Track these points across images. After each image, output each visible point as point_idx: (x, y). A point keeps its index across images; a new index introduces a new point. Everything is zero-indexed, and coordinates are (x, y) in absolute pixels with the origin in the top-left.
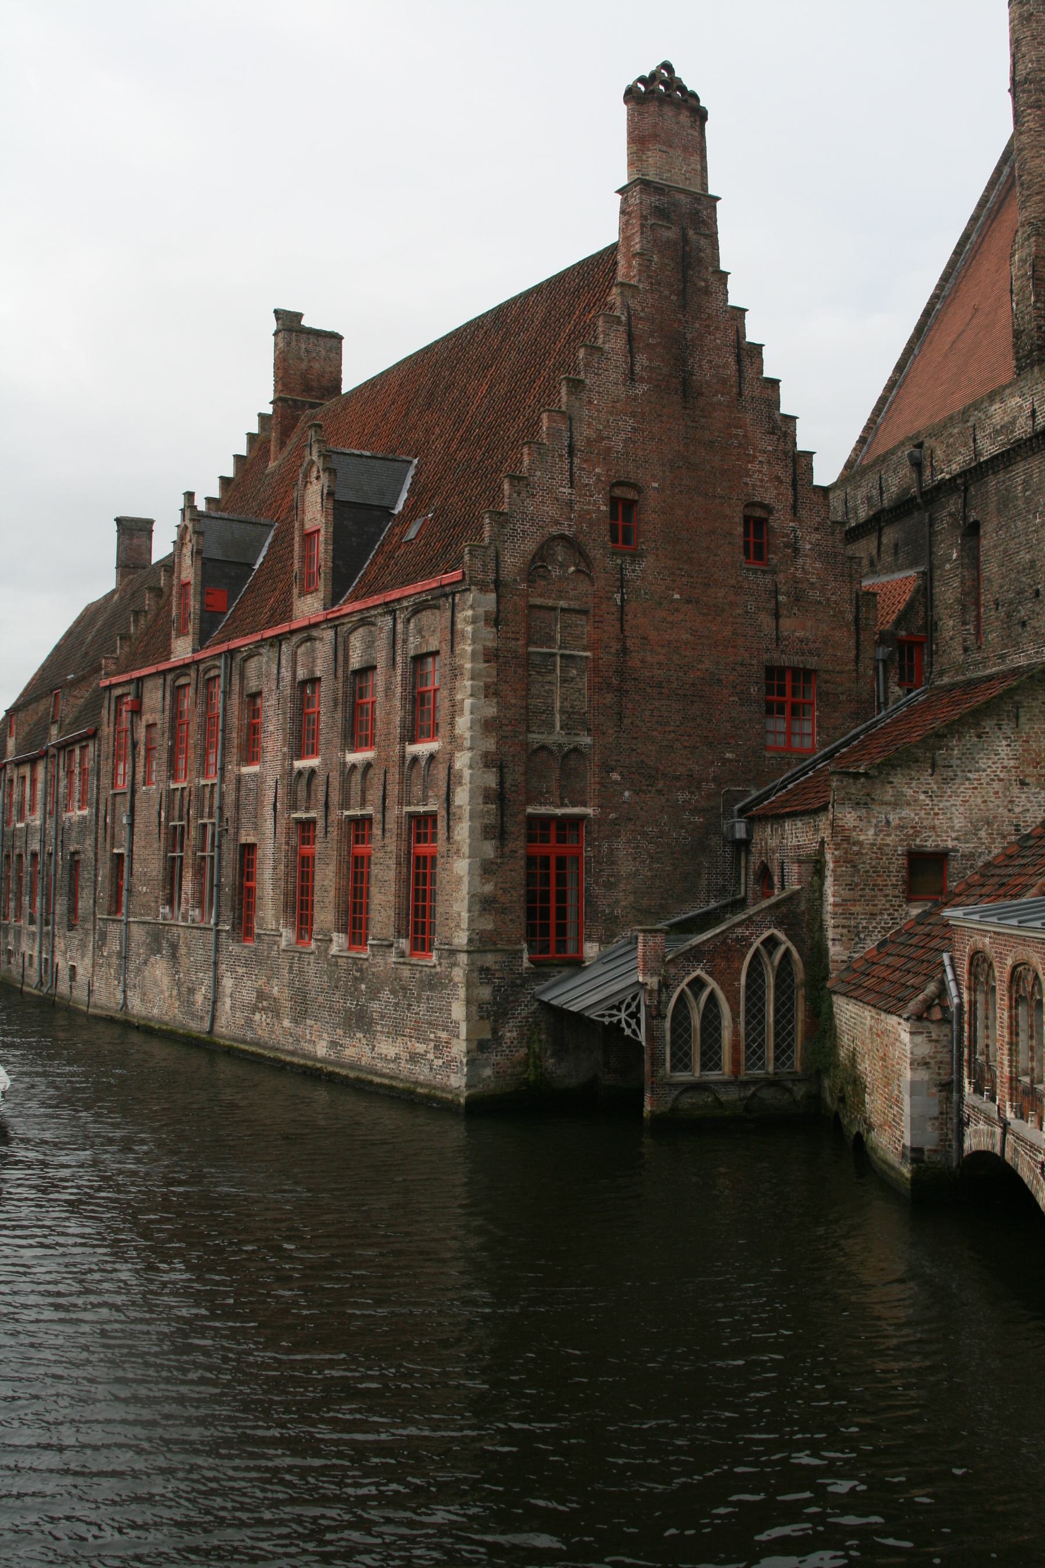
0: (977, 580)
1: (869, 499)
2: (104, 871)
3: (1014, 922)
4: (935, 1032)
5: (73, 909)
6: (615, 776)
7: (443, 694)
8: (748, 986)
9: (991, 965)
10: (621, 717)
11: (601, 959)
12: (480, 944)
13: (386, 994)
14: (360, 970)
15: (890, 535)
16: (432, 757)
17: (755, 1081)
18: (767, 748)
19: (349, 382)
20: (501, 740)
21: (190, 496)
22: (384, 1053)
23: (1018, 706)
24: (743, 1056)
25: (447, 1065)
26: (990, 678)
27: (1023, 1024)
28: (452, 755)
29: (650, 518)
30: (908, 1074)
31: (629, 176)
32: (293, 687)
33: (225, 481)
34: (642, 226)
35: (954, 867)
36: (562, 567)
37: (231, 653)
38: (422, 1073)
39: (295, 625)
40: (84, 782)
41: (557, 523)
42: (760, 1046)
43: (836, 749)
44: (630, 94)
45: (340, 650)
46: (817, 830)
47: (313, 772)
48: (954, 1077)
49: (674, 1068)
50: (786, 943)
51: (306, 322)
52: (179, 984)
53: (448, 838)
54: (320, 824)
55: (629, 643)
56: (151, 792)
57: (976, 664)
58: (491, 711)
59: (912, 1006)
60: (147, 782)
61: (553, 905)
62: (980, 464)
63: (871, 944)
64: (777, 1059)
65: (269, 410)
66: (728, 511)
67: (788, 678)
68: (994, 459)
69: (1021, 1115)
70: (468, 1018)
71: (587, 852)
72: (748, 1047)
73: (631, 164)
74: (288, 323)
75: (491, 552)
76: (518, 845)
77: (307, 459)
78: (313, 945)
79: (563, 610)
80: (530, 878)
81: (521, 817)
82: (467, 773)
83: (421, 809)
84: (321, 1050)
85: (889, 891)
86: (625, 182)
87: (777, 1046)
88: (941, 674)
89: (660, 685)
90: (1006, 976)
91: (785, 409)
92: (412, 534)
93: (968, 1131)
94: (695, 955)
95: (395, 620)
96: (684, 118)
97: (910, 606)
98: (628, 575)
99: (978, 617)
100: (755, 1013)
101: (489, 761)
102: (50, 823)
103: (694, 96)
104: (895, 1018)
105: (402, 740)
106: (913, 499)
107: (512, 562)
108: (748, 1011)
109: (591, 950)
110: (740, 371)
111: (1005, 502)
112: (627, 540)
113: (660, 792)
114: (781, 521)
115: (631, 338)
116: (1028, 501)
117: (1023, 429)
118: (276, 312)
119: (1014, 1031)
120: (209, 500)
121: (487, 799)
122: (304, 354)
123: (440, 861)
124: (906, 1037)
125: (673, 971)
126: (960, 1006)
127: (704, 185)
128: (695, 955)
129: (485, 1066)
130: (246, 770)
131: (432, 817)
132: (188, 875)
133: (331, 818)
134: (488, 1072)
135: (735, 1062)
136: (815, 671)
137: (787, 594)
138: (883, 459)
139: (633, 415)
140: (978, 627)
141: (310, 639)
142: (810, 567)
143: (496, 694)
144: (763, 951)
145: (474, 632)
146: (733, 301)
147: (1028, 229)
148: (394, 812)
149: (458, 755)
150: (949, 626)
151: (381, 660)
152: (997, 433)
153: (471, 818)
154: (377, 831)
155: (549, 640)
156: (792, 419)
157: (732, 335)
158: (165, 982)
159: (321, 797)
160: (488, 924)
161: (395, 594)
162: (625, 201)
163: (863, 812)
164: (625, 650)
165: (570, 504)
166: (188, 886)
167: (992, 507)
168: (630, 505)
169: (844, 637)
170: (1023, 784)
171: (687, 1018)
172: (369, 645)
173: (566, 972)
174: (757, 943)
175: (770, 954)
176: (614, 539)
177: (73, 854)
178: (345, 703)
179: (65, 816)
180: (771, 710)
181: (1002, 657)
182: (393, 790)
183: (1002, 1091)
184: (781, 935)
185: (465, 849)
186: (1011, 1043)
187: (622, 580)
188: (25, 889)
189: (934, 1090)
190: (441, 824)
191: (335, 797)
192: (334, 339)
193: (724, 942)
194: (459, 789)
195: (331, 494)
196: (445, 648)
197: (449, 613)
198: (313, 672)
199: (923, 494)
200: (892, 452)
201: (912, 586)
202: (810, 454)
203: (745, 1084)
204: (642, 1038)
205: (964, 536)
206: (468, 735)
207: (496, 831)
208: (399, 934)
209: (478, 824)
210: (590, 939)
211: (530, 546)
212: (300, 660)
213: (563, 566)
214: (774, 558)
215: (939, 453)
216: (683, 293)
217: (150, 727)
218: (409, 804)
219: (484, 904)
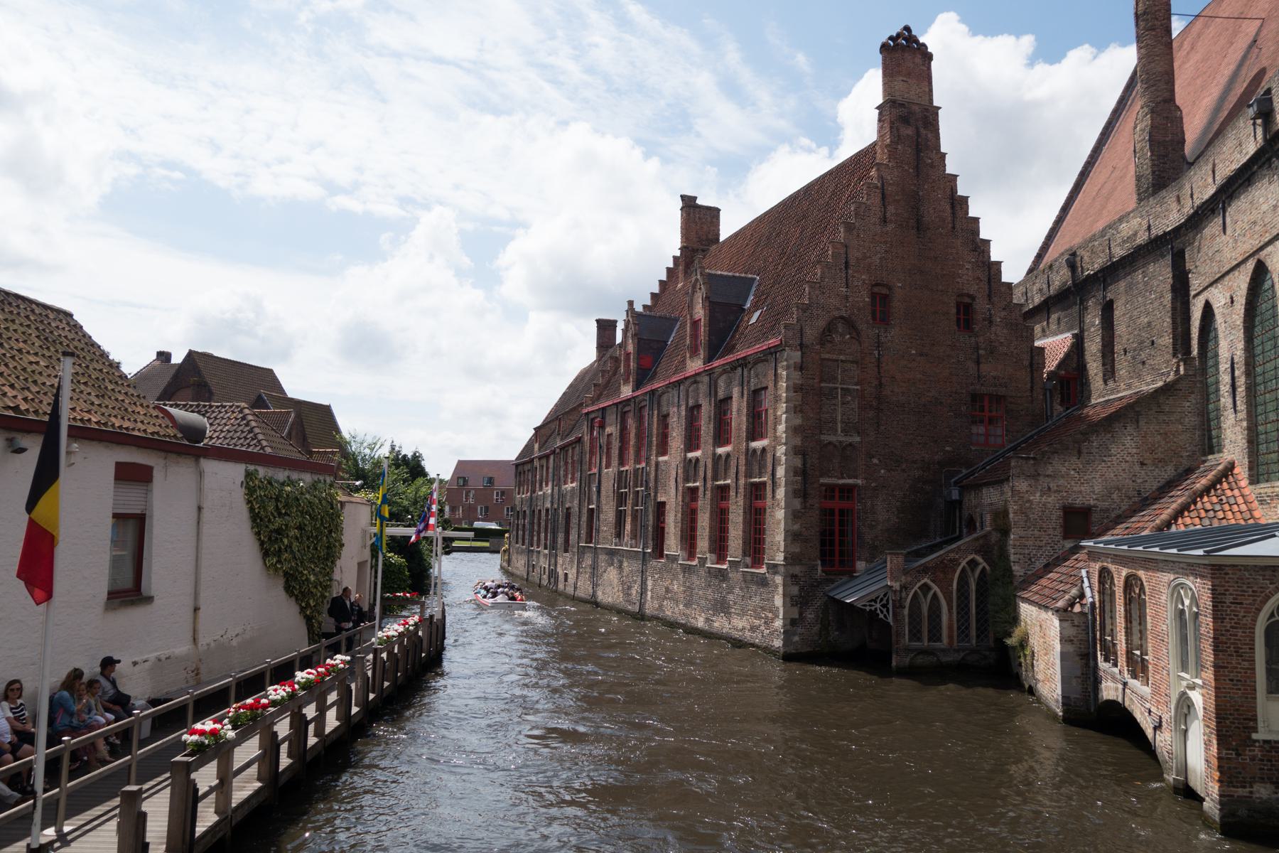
1: (1041, 290)
2: (584, 518)
5: (567, 540)
6: (875, 461)
7: (770, 411)
8: (958, 590)
11: (868, 572)
13: (737, 591)
16: (764, 450)
19: (724, 234)
21: (631, 303)
22: (737, 625)
23: (1138, 414)
24: (955, 634)
25: (771, 633)
27: (1135, 615)
31: (884, 96)
33: (653, 295)
35: (1095, 517)
37: (653, 392)
40: (573, 467)
41: (838, 309)
43: (1019, 445)
44: (884, 48)
45: (713, 387)
46: (1002, 493)
47: (697, 460)
48: (1091, 650)
49: (910, 640)
50: (983, 564)
51: (699, 202)
52: (623, 583)
54: (701, 489)
55: (883, 380)
56: (610, 472)
58: (798, 421)
60: (608, 466)
61: (837, 538)
62: (1113, 263)
64: (978, 636)
65: (678, 253)
68: (1123, 259)
70: (784, 606)
71: (858, 506)
72: (959, 628)
73: (885, 91)
74: (689, 203)
75: (798, 327)
81: (816, 485)
82: (783, 458)
84: (700, 623)
85: (1051, 532)
87: (978, 629)
91: (983, 235)
92: (753, 320)
94: (925, 570)
96: (918, 59)
97: (1067, 355)
98: (883, 339)
101: (795, 451)
102: (556, 489)
106: (1069, 288)
107: (811, 334)
108: (958, 606)
109: (861, 565)
111: (1130, 287)
113: (904, 470)
114: (981, 306)
115: (884, 197)
116: (1146, 284)
117: (1142, 238)
120: (645, 307)
121: (796, 474)
122: (698, 218)
125: (909, 579)
126: (1093, 604)
127: (931, 100)
128: (925, 570)
129: (794, 634)
130: (661, 459)
132: (629, 520)
134: (796, 638)
135: (951, 637)
137: (985, 349)
139: (886, 242)
141: (696, 382)
143: (801, 411)
144: (968, 569)
147: (1146, 110)
148: (742, 481)
150: (1094, 367)
151: (736, 392)
152: (1124, 242)
154: (732, 493)
155: (834, 379)
156: (987, 242)
157: (948, 192)
158: (616, 581)
159: (702, 474)
160: (796, 549)
162: (880, 114)
164: (881, 384)
165: (847, 297)
166: (628, 527)
168: (885, 297)
170: (1142, 464)
171: (919, 608)
173: (845, 578)
174: (964, 563)
175: (973, 571)
176: (874, 319)
177: (568, 509)
179: (564, 487)
182: (742, 469)
185: (783, 504)
186: (1126, 628)
187: (878, 342)
188: (542, 530)
189: (1077, 658)
190: (769, 489)
192: (718, 210)
193: (942, 562)
196: (771, 385)
200: (1056, 260)
201: (1069, 343)
202: (999, 263)
203: (958, 651)
204: (890, 620)
205: (1103, 310)
210: (860, 559)
211: (821, 323)
213: (842, 335)
214: (976, 328)
216: (917, 168)
217: (609, 435)
219: (792, 537)
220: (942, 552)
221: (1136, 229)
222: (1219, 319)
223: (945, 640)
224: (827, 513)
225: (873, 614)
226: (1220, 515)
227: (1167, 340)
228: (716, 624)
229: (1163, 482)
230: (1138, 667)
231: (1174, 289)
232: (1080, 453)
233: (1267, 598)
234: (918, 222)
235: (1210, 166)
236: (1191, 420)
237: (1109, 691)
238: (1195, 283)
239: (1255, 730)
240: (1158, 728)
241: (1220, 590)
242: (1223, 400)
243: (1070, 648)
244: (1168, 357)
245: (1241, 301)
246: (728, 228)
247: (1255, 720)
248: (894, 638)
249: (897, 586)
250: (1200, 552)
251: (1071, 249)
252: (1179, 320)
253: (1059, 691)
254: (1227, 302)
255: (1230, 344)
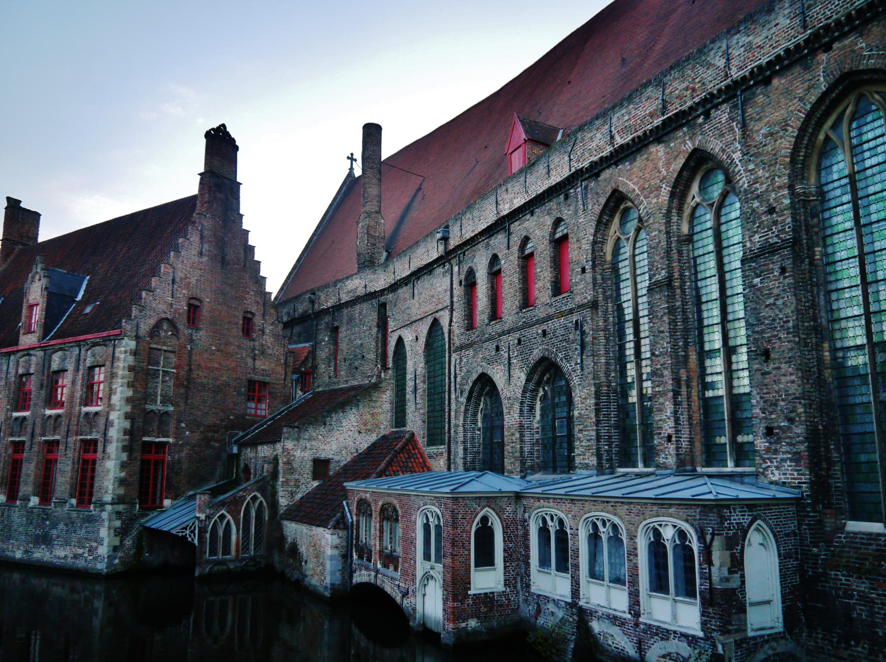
0: (336, 351)
1: (288, 313)
3: (386, 487)
4: (341, 533)
6: (183, 425)
9: (369, 505)
10: (187, 399)
11: (173, 507)
12: (118, 500)
13: (61, 526)
14: (47, 514)
15: (297, 329)
16: (96, 413)
17: (245, 558)
18: (248, 415)
20: (134, 407)
23: (359, 401)
25: (96, 559)
26: (341, 389)
28: (108, 413)
29: (205, 312)
30: (329, 552)
32: (15, 377)
34: (210, 191)
35: (332, 466)
36: (166, 332)
38: (81, 564)
39: (20, 348)
42: (248, 544)
44: (208, 135)
46: (275, 450)
47: (24, 418)
51: (22, 205)
53: (104, 451)
54: (27, 444)
55: (193, 367)
57: (334, 383)
58: (130, 393)
59: (331, 523)
61: (151, 482)
63: (298, 496)
66: (237, 314)
67: (257, 385)
69: (385, 566)
73: (206, 164)
74: (13, 205)
75: (135, 322)
76: (138, 455)
77: (34, 271)
78: (18, 502)
79: (165, 351)
80: (142, 471)
81: (140, 442)
83: (89, 437)
84: (18, 555)
85: (305, 476)
86: (202, 170)
88: (318, 386)
89: (204, 386)
90: (378, 509)
91: (262, 274)
92: (88, 310)
93: (355, 575)
94: (222, 504)
95: (80, 350)
98: (194, 338)
99: (336, 365)
100: (246, 530)
101: (127, 416)
103: (234, 140)
104: (321, 529)
105: (80, 405)
109: (167, 503)
110: (245, 256)
111: (351, 320)
112: (193, 323)
114: (258, 321)
115: (202, 238)
116: (360, 320)
117: (361, 291)
118: (8, 199)
119: (381, 531)
123: (98, 462)
124: (329, 537)
128: (222, 504)
129: (115, 558)
131: (95, 442)
133: (34, 441)
134: (117, 561)
135: (237, 551)
136: (268, 383)
138: (297, 298)
139: (201, 269)
140: (335, 369)
142: (268, 340)
143: (133, 386)
145: (125, 358)
146: (244, 227)
149: (112, 413)
150: (322, 367)
151: (71, 367)
153: (117, 441)
159: (29, 429)
160: (121, 491)
161: (82, 337)
162: (201, 179)
163: (296, 443)
164: (190, 370)
165: (171, 305)
167: (345, 321)
168: (196, 308)
169: (280, 370)
170: (360, 432)
171: (217, 532)
172: (64, 359)
174: (248, 499)
176: (189, 322)
178: (47, 386)
180: (250, 399)
181: (347, 381)
183: (375, 557)
184: (259, 495)
185: (113, 456)
191: (38, 431)
193: (234, 498)
194: (111, 429)
195: (46, 288)
196: (108, 364)
197: (111, 349)
198: (28, 370)
199: (314, 313)
200: (301, 295)
203: (241, 561)
204: (196, 542)
205: (331, 332)
206: (118, 404)
207: (128, 448)
208: (71, 496)
209: (120, 445)
210: (167, 498)
211: (152, 322)
212: (21, 364)
213: (166, 331)
214: (254, 335)
215: (323, 297)
218: (81, 435)
220: (235, 491)
221: (356, 285)
222: (408, 348)
223: (233, 553)
224: (145, 464)
225: (184, 537)
226: (410, 465)
227: (372, 356)
228: (35, 555)
229: (370, 444)
230: (390, 559)
231: (378, 326)
232: (325, 424)
233: (477, 514)
234: (223, 258)
235: (407, 258)
236: (387, 406)
237: (361, 577)
238: (391, 325)
239: (470, 589)
240: (405, 594)
241: (456, 511)
242: (407, 396)
243: (336, 552)
244: (373, 366)
245: (422, 340)
246: (46, 233)
247: (470, 583)
248: (198, 555)
249: (203, 516)
250: (448, 490)
251: (312, 290)
252: (380, 345)
253: (328, 580)
254: (414, 340)
255: (415, 363)
